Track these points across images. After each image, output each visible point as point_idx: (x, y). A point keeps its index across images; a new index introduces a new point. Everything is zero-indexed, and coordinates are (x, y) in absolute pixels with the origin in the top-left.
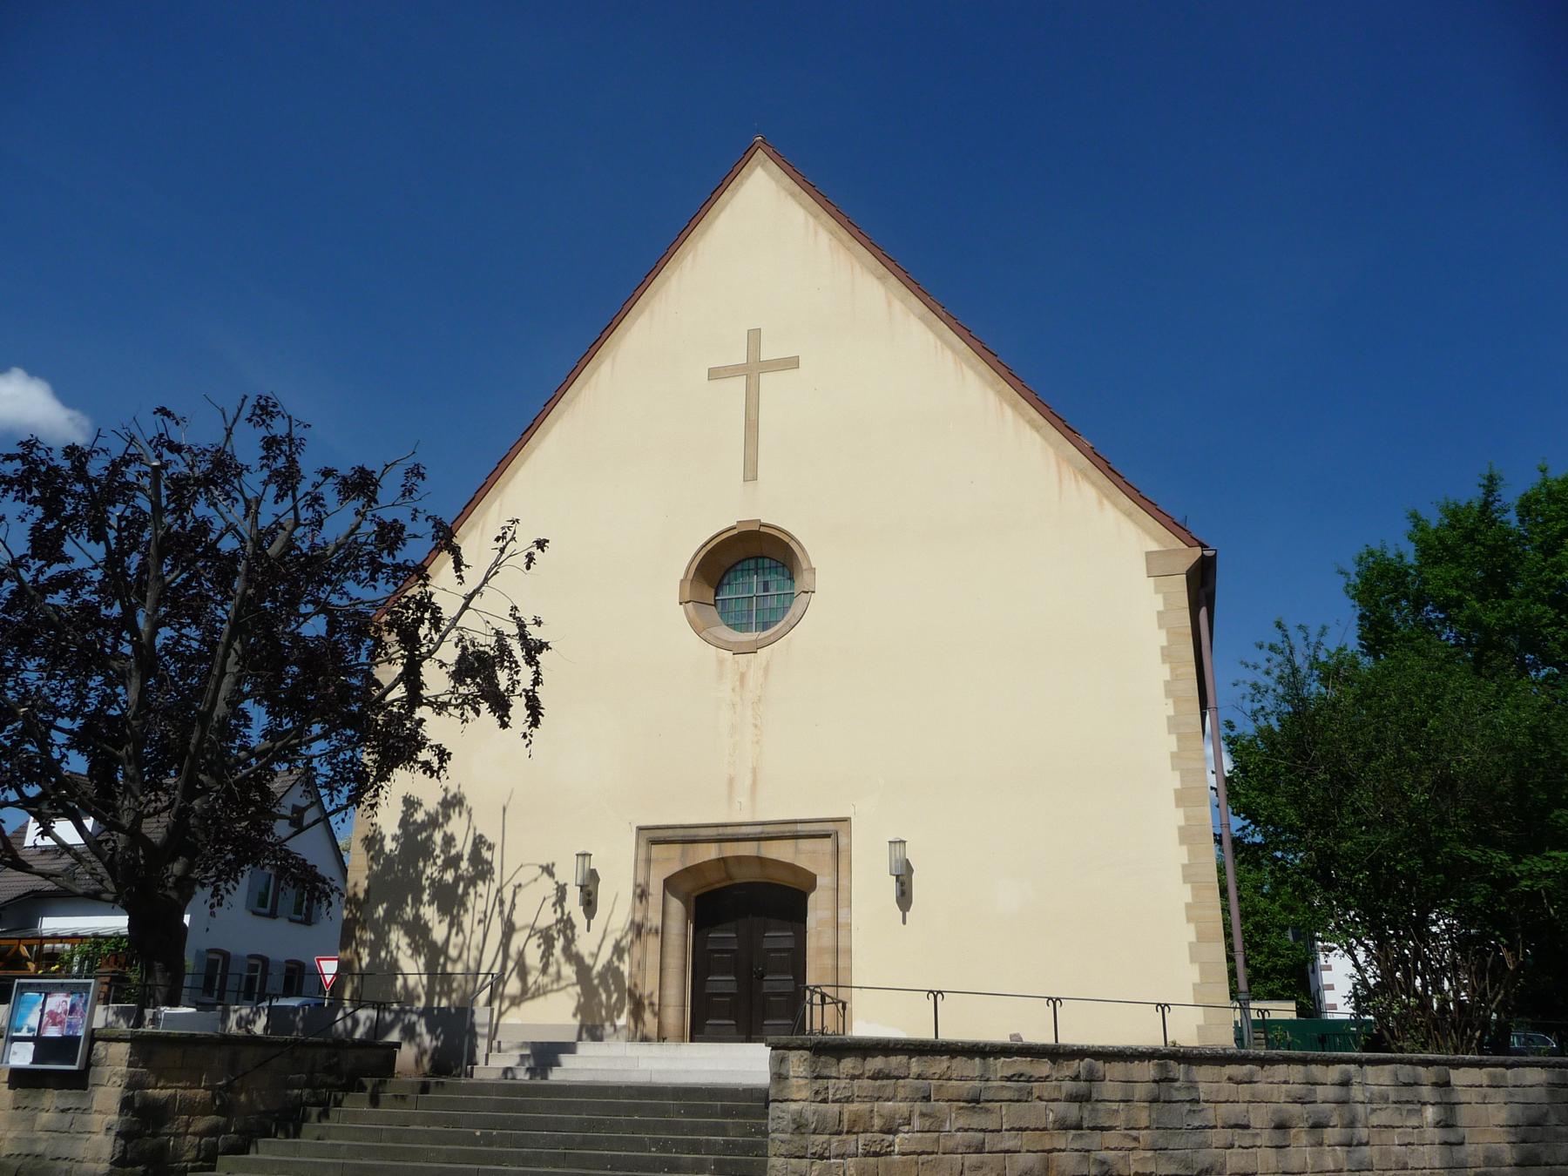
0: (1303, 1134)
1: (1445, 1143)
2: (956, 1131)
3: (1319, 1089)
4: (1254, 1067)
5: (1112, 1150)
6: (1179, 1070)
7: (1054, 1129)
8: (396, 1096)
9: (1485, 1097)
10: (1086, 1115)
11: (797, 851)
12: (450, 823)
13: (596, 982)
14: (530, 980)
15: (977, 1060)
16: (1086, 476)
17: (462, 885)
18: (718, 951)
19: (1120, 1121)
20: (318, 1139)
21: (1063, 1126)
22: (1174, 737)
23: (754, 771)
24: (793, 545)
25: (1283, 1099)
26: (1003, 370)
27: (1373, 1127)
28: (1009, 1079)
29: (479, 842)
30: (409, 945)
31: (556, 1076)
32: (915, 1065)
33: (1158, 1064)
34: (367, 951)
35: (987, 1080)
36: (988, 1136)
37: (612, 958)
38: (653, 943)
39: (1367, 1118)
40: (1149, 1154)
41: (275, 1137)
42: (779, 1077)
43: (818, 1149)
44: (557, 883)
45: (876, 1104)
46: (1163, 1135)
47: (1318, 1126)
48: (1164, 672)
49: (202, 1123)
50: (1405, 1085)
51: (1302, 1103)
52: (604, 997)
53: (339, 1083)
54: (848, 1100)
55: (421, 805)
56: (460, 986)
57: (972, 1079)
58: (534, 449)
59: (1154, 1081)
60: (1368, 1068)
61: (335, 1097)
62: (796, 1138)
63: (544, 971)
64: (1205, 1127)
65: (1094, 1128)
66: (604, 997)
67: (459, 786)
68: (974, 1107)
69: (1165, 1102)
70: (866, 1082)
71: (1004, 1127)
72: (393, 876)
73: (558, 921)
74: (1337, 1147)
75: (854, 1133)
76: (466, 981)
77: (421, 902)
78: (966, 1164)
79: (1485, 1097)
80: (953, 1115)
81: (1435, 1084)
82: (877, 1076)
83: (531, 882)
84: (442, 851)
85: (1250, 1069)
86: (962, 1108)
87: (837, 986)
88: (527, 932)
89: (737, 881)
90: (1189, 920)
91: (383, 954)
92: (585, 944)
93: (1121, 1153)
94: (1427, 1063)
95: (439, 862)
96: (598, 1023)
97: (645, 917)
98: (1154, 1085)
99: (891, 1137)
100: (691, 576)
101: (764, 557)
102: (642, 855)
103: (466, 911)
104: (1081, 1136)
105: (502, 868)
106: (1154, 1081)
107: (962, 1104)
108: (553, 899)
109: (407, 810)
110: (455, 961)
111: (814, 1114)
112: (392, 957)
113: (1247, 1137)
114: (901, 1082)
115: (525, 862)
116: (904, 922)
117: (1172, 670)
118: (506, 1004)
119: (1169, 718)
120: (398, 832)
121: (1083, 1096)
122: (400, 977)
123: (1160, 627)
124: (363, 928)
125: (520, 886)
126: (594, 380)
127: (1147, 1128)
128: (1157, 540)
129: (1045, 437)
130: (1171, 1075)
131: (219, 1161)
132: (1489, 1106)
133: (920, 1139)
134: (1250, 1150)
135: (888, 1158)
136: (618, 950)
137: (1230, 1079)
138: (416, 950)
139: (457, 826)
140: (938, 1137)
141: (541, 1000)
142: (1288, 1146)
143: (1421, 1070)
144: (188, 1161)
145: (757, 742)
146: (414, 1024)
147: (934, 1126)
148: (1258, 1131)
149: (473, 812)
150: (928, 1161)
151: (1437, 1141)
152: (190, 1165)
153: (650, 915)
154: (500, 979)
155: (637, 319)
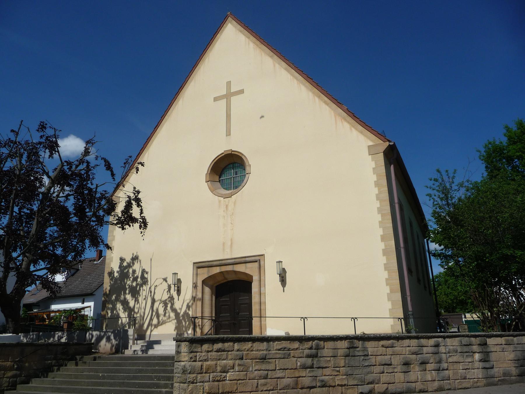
0: (417, 367)
1: (484, 368)
2: (255, 371)
3: (425, 349)
4: (394, 341)
5: (327, 376)
6: (359, 344)
7: (300, 369)
8: (83, 362)
9: (503, 349)
10: (315, 363)
11: (246, 268)
12: (134, 266)
13: (181, 318)
14: (160, 319)
15: (265, 343)
16: (345, 120)
17: (138, 287)
18: (223, 305)
19: (331, 364)
20: (53, 378)
21: (304, 367)
22: (380, 215)
23: (231, 240)
24: (243, 157)
25: (407, 353)
26: (315, 85)
27: (450, 363)
28: (279, 350)
29: (144, 271)
30: (123, 308)
31: (151, 352)
32: (236, 346)
33: (349, 342)
34: (110, 311)
35: (270, 351)
36: (270, 372)
37: (186, 309)
38: (199, 303)
39: (447, 359)
40: (344, 377)
41: (41, 378)
42: (178, 352)
43: (191, 380)
44: (168, 284)
45: (218, 361)
46: (351, 369)
47: (424, 363)
48: (376, 191)
49: (10, 374)
50: (465, 345)
51: (417, 354)
52: (184, 323)
53: (68, 358)
54: (206, 360)
55: (125, 260)
56: (138, 322)
57: (262, 350)
58: (158, 133)
59: (347, 348)
60: (448, 340)
61: (65, 363)
62: (183, 376)
63: (165, 315)
64: (370, 366)
65: (318, 368)
66: (184, 323)
67: (137, 253)
68: (263, 361)
69: (352, 356)
70: (214, 353)
71: (277, 369)
72: (117, 285)
73: (169, 298)
74: (433, 372)
75: (208, 373)
76: (140, 320)
77: (126, 293)
78: (259, 384)
79: (503, 349)
80: (254, 365)
81: (479, 345)
82: (218, 351)
83: (160, 284)
84: (132, 276)
85: (392, 342)
86: (257, 362)
87: (261, 317)
88: (159, 302)
89: (229, 280)
90: (387, 285)
91: (115, 312)
92: (177, 305)
93: (331, 377)
94: (475, 336)
95: (131, 279)
96: (182, 333)
97: (196, 295)
98: (347, 350)
99: (225, 374)
100: (209, 172)
101: (235, 163)
102: (195, 273)
103: (140, 296)
104: (313, 371)
105: (151, 280)
106: (347, 348)
107: (257, 360)
108: (167, 290)
109: (121, 262)
110: (137, 313)
111: (190, 366)
112: (117, 313)
113: (390, 369)
114: (230, 353)
115: (158, 278)
116: (284, 291)
117: (379, 189)
118: (153, 327)
119: (378, 208)
120: (118, 270)
121: (314, 355)
122: (120, 319)
123: (374, 174)
124: (109, 304)
125: (156, 286)
126: (177, 107)
127: (343, 367)
128: (372, 141)
129: (330, 107)
130: (355, 345)
131: (17, 387)
132: (505, 352)
133: (239, 374)
134: (392, 374)
135: (224, 382)
136: (188, 307)
137: (383, 346)
138: (125, 310)
139: (137, 267)
140: (247, 373)
141: (164, 325)
142: (410, 372)
143: (473, 339)
144: (5, 387)
145: (232, 229)
146: (110, 336)
147: (245, 369)
148: (396, 366)
149: (141, 261)
150: (242, 383)
151: (480, 367)
152: (5, 388)
153: (198, 293)
154: (151, 319)
155: (190, 83)
